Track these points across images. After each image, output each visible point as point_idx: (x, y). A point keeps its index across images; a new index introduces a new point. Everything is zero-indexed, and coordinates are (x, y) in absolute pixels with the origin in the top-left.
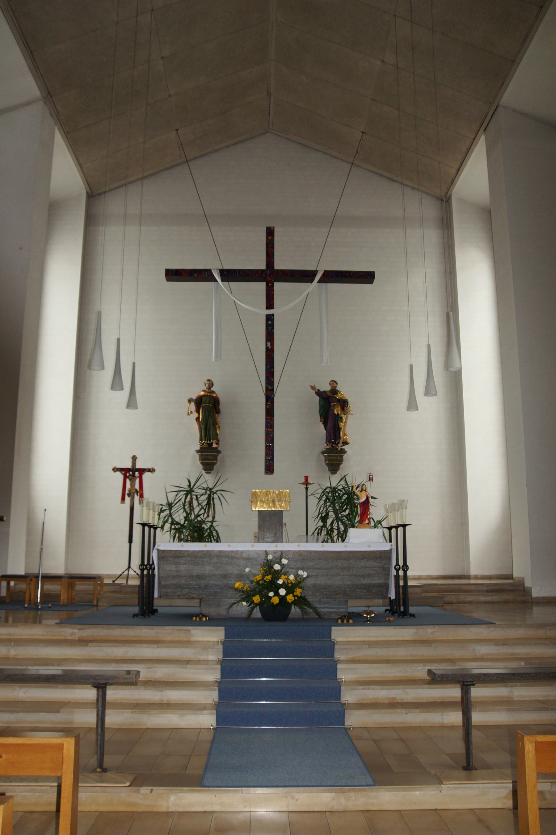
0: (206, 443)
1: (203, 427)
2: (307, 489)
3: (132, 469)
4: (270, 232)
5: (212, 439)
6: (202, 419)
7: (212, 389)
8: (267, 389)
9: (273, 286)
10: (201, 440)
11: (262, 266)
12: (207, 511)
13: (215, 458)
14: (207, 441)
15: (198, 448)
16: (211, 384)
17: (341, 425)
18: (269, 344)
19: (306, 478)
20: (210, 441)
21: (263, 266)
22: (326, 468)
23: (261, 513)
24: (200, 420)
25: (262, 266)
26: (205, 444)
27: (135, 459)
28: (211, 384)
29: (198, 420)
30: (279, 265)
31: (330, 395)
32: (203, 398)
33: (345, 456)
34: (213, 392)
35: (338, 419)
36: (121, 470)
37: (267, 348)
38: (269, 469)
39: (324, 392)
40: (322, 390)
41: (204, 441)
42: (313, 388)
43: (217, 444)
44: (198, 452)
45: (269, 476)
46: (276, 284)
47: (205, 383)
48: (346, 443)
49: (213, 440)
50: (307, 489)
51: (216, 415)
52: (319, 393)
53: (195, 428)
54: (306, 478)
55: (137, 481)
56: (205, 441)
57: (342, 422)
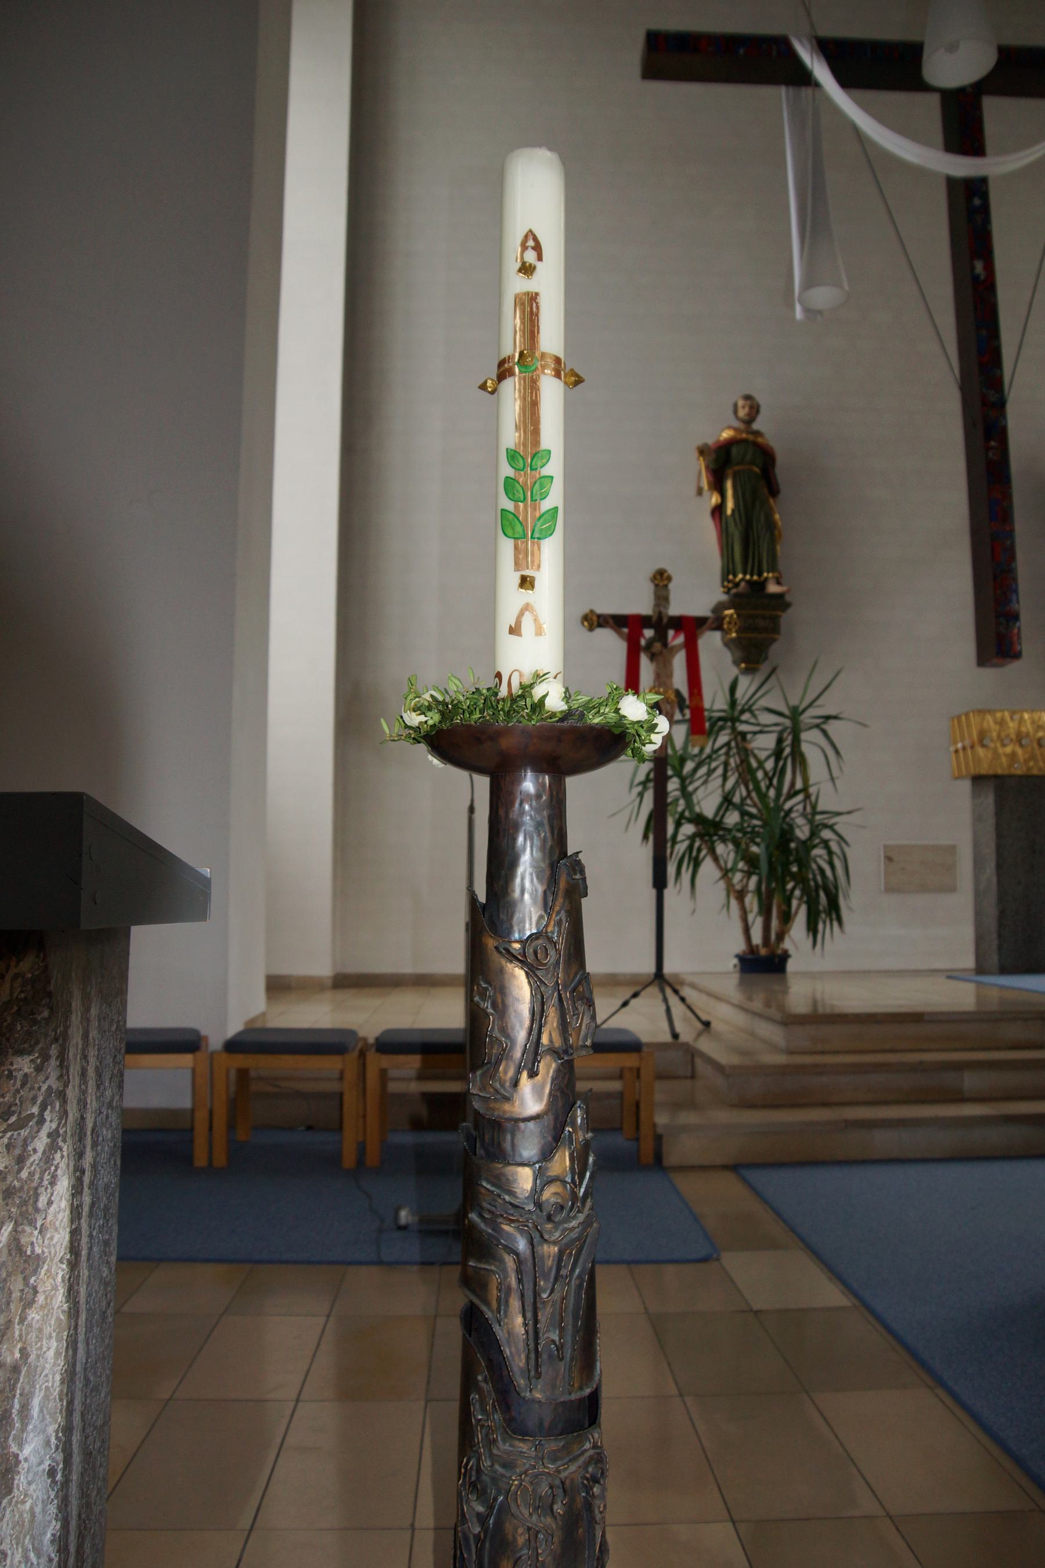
0: (748, 582)
1: (736, 533)
3: (654, 619)
5: (765, 566)
6: (733, 511)
12: (775, 781)
14: (752, 575)
20: (760, 574)
24: (729, 512)
26: (743, 584)
27: (665, 582)
29: (717, 515)
32: (734, 450)
34: (758, 433)
36: (617, 622)
41: (740, 576)
47: (735, 406)
49: (768, 572)
51: (771, 501)
55: (679, 662)
56: (745, 574)
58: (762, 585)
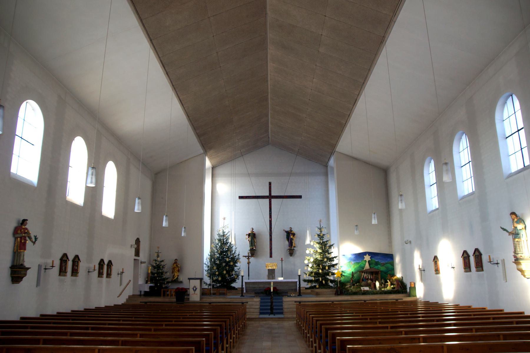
2: (282, 262)
4: (270, 184)
7: (253, 231)
8: (270, 233)
9: (271, 200)
10: (250, 247)
11: (268, 194)
13: (254, 252)
15: (249, 249)
16: (253, 229)
17: (293, 241)
18: (270, 219)
19: (282, 258)
21: (268, 195)
22: (289, 255)
23: (269, 270)
25: (268, 194)
28: (253, 229)
30: (273, 194)
31: (290, 232)
33: (294, 251)
34: (253, 232)
35: (292, 239)
37: (270, 220)
38: (271, 256)
39: (288, 231)
40: (287, 230)
42: (284, 230)
43: (255, 248)
44: (249, 250)
45: (271, 258)
46: (272, 200)
48: (294, 247)
50: (282, 262)
52: (286, 232)
53: (248, 243)
54: (282, 258)
57: (293, 240)
58: (253, 248)
